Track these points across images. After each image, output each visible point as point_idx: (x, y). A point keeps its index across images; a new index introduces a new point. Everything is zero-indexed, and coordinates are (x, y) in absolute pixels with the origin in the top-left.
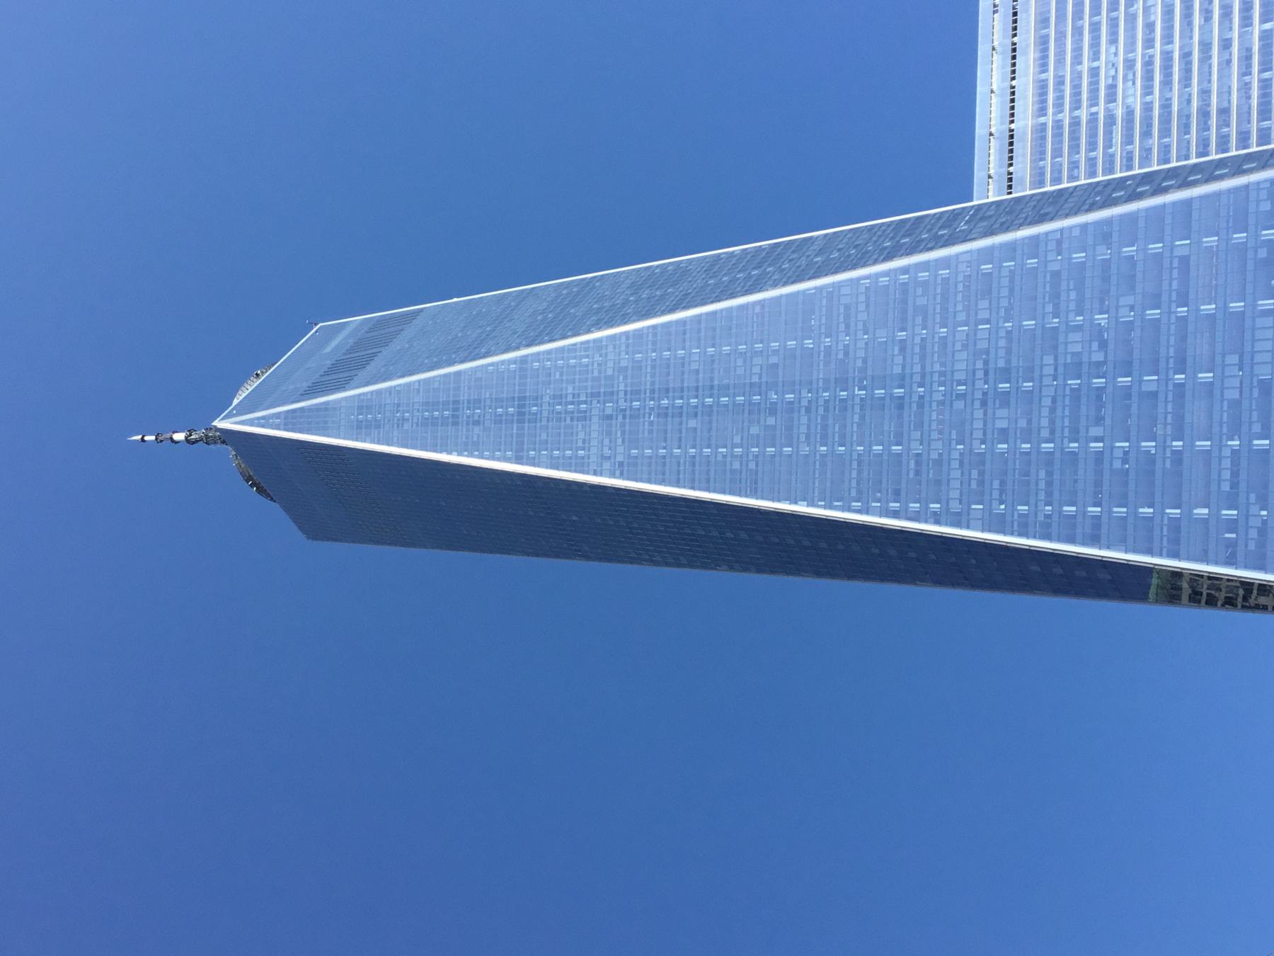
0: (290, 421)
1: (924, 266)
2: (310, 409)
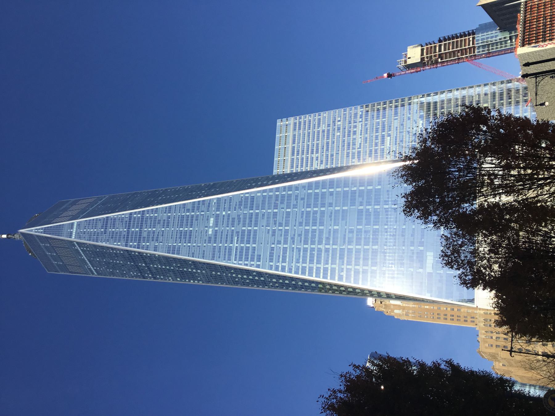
0: (46, 231)
1: (259, 192)
2: (54, 227)
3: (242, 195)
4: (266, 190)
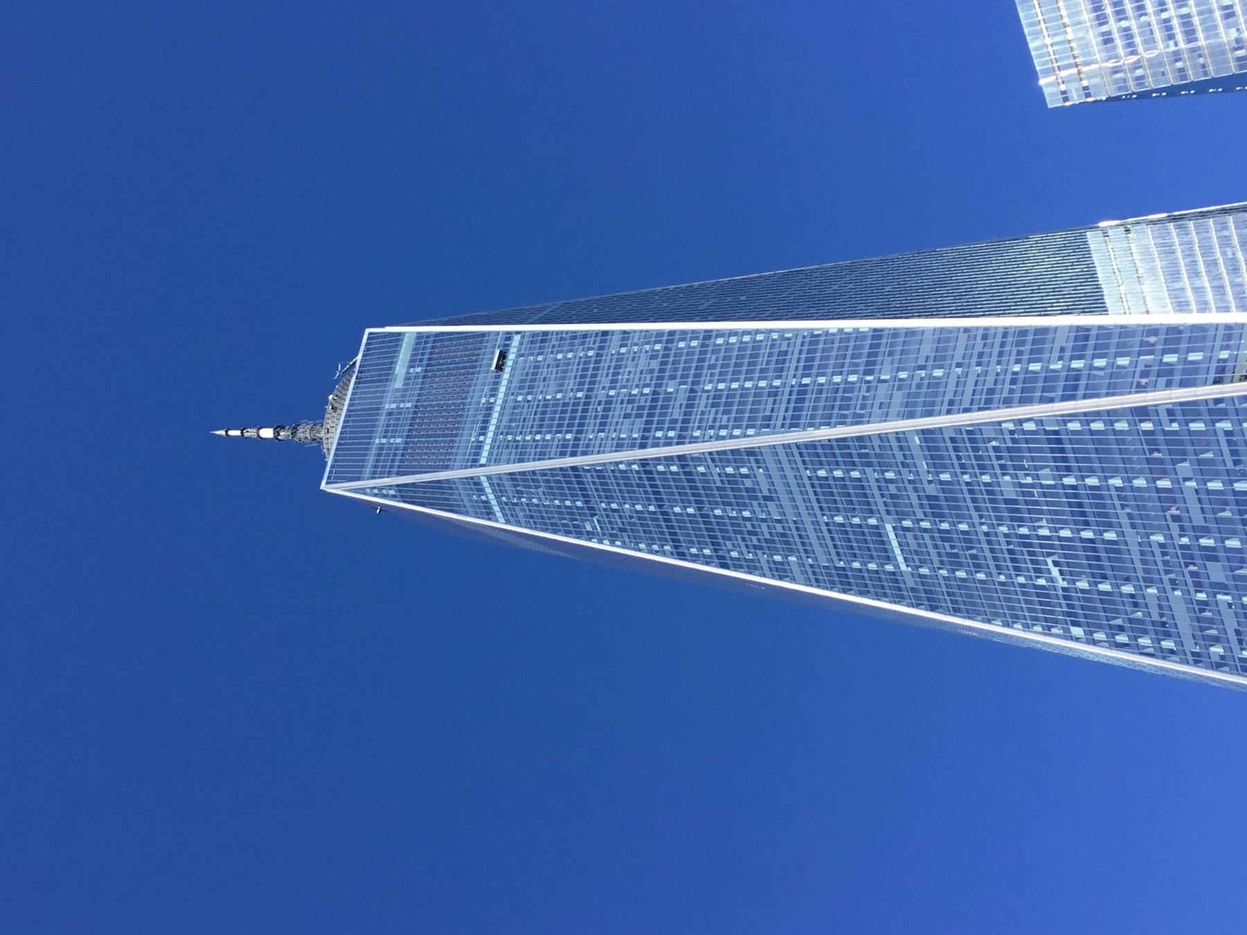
0: (404, 492)
3: (1011, 426)
4: (1098, 413)
